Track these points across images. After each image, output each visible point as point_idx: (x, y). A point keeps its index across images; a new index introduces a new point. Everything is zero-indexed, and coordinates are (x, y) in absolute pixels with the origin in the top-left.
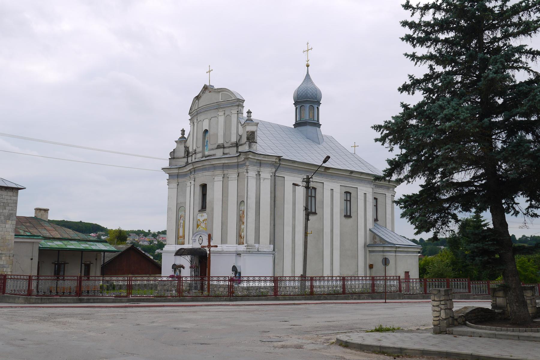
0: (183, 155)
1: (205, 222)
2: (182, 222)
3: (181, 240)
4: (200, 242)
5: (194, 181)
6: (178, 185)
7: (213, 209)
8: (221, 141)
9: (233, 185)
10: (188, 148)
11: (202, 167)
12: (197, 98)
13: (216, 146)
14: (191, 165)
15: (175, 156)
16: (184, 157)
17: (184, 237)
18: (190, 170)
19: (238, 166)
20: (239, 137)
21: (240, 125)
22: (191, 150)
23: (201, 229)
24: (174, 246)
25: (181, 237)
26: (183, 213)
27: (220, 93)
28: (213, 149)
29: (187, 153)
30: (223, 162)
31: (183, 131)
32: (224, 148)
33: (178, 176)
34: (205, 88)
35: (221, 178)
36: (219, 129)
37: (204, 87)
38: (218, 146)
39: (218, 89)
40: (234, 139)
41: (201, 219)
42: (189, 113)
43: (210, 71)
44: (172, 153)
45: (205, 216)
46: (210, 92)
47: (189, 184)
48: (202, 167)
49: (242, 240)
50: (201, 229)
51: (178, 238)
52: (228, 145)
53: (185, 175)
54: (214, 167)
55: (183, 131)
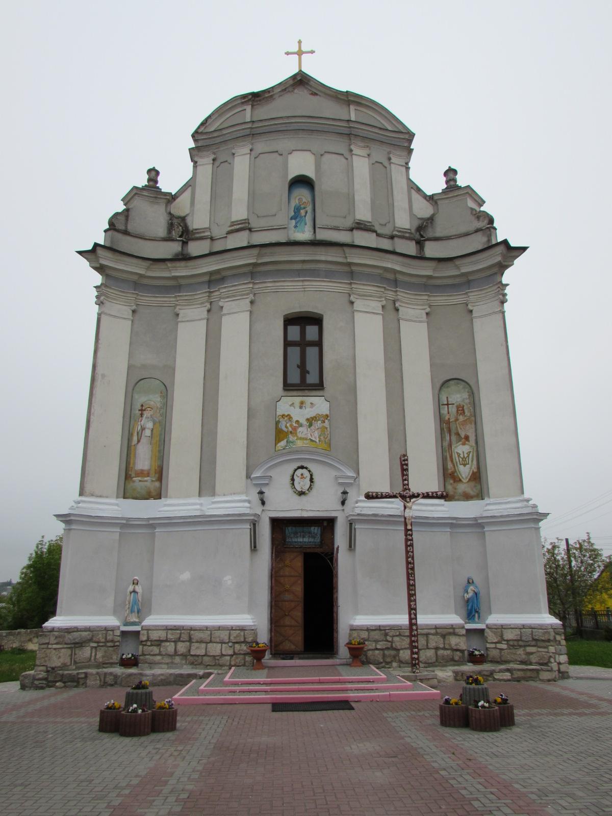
0: (162, 232)
1: (319, 424)
2: (150, 425)
3: (139, 484)
4: (302, 484)
5: (252, 302)
6: (134, 312)
7: (353, 390)
8: (363, 214)
9: (415, 337)
10: (183, 219)
11: (299, 267)
12: (255, 98)
13: (349, 223)
14: (255, 251)
15: (130, 228)
16: (168, 239)
17: (160, 474)
18: (211, 273)
19: (427, 286)
20: (416, 223)
21: (415, 195)
22: (198, 222)
23: (299, 443)
24: (114, 501)
25: (141, 473)
26: (155, 400)
27: (352, 107)
28: (336, 229)
29: (181, 230)
30: (389, 265)
31: (153, 174)
32: (378, 235)
33: (138, 285)
34: (301, 81)
35: (376, 305)
36: (357, 186)
37: (294, 77)
38: (357, 223)
39: (348, 93)
40: (403, 221)
41: (300, 415)
42: (195, 135)
43: (300, 53)
44: (122, 218)
45: (318, 405)
46: (315, 94)
47: (202, 312)
48: (299, 267)
49: (462, 488)
50: (299, 443)
51: (128, 477)
52: (387, 231)
53: (176, 287)
54: (351, 273)
55: (153, 174)
